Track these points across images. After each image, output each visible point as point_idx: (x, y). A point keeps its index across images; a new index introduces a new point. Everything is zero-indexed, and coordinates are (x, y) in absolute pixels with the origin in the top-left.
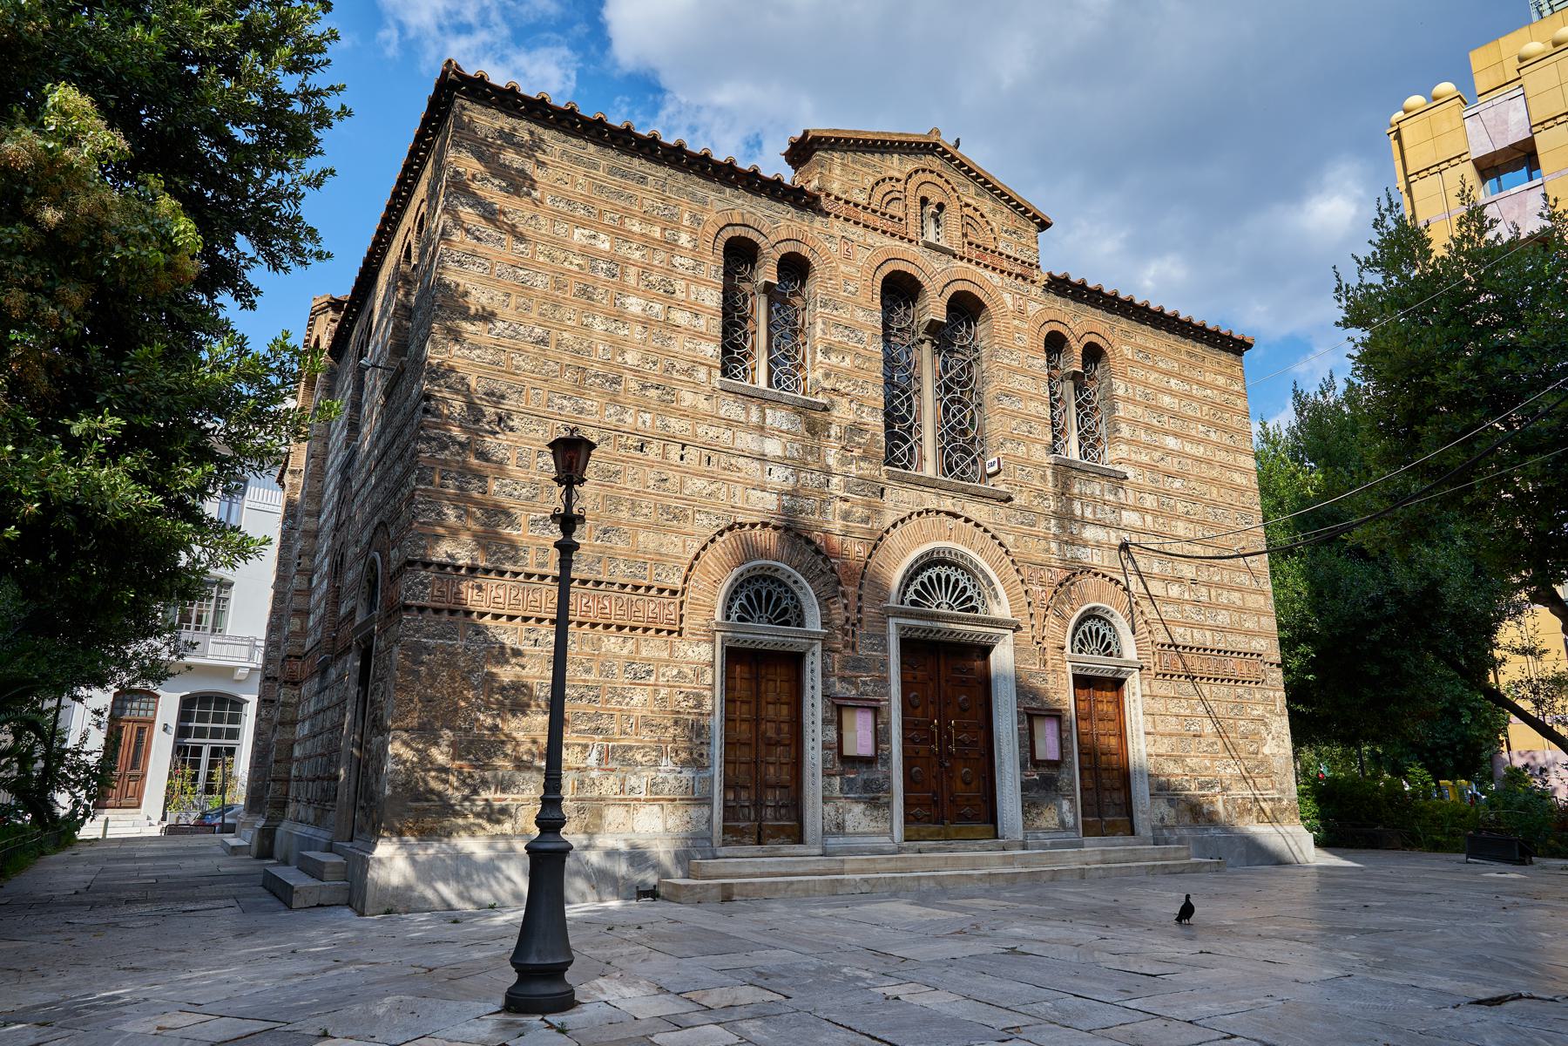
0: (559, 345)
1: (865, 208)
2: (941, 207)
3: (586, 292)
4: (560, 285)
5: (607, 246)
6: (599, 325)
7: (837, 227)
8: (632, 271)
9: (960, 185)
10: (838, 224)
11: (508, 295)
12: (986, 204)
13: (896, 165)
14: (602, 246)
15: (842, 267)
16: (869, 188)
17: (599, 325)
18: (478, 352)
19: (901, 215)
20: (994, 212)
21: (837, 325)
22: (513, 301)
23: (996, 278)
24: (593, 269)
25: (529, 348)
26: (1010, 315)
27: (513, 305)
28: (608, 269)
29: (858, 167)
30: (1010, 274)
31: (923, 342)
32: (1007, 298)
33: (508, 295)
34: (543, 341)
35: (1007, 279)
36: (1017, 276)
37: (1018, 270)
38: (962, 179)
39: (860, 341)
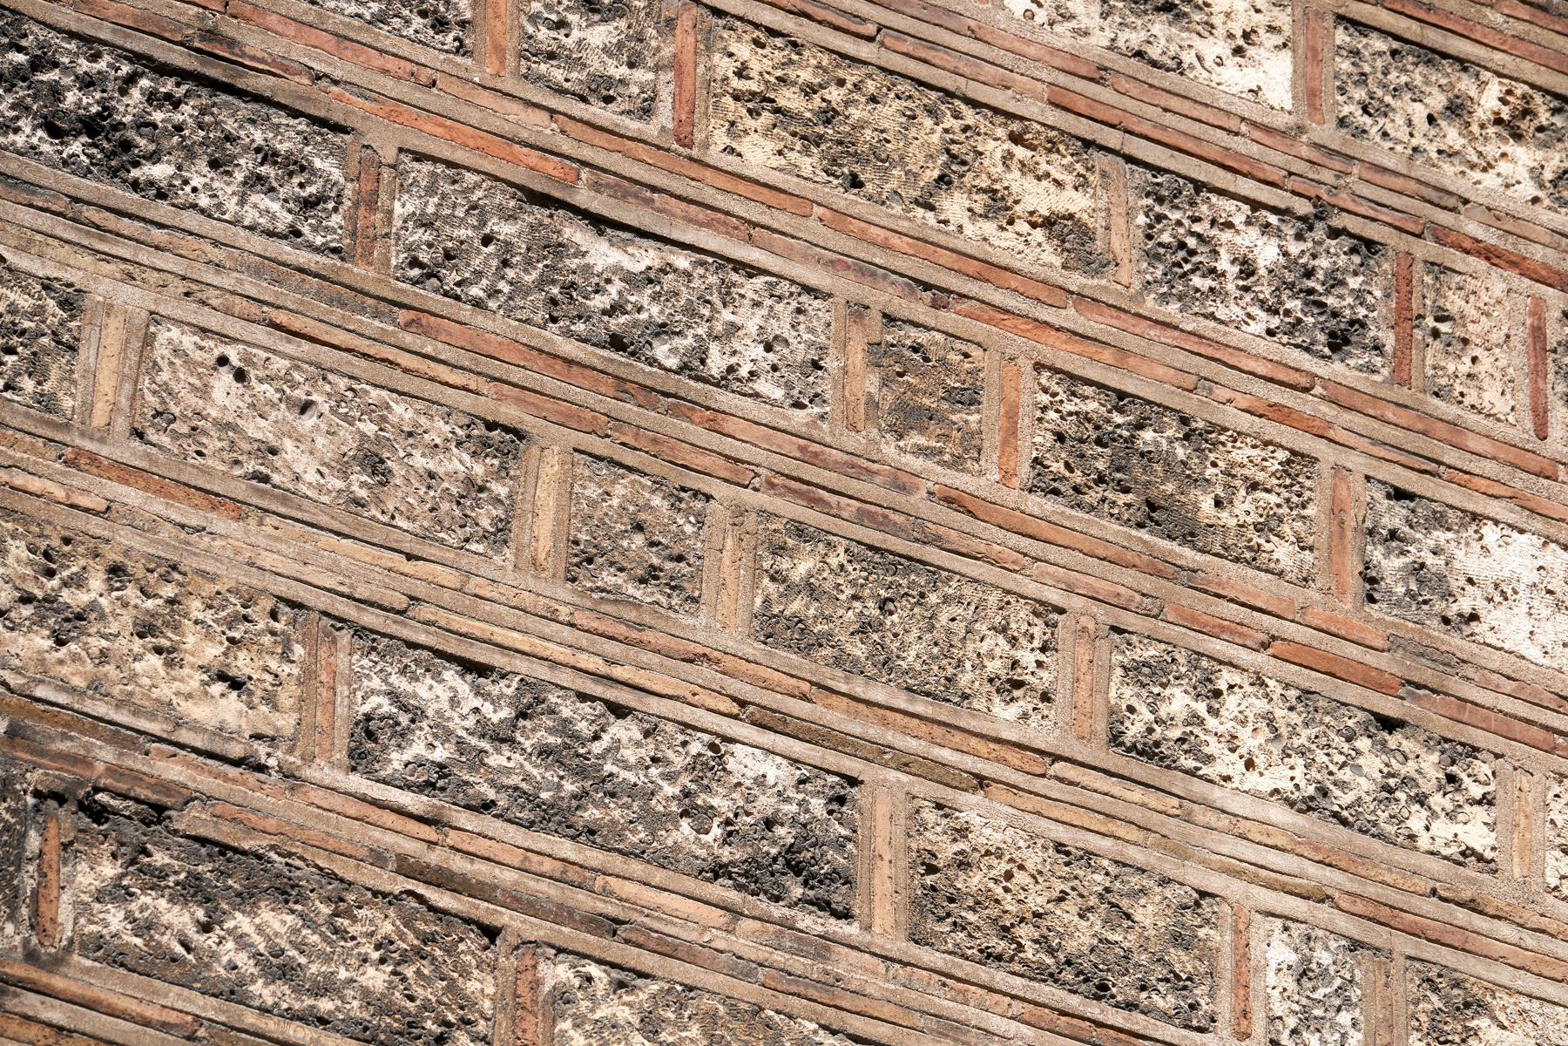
0: (934, 898)
3: (1123, 460)
4: (926, 393)
5: (1272, 78)
6: (1253, 762)
8: (1490, 302)
11: (502, 441)
14: (1234, 78)
17: (1253, 762)
18: (275, 921)
22: (546, 493)
24: (1179, 262)
25: (687, 911)
27: (542, 531)
28: (1297, 278)
33: (502, 441)
34: (795, 869)
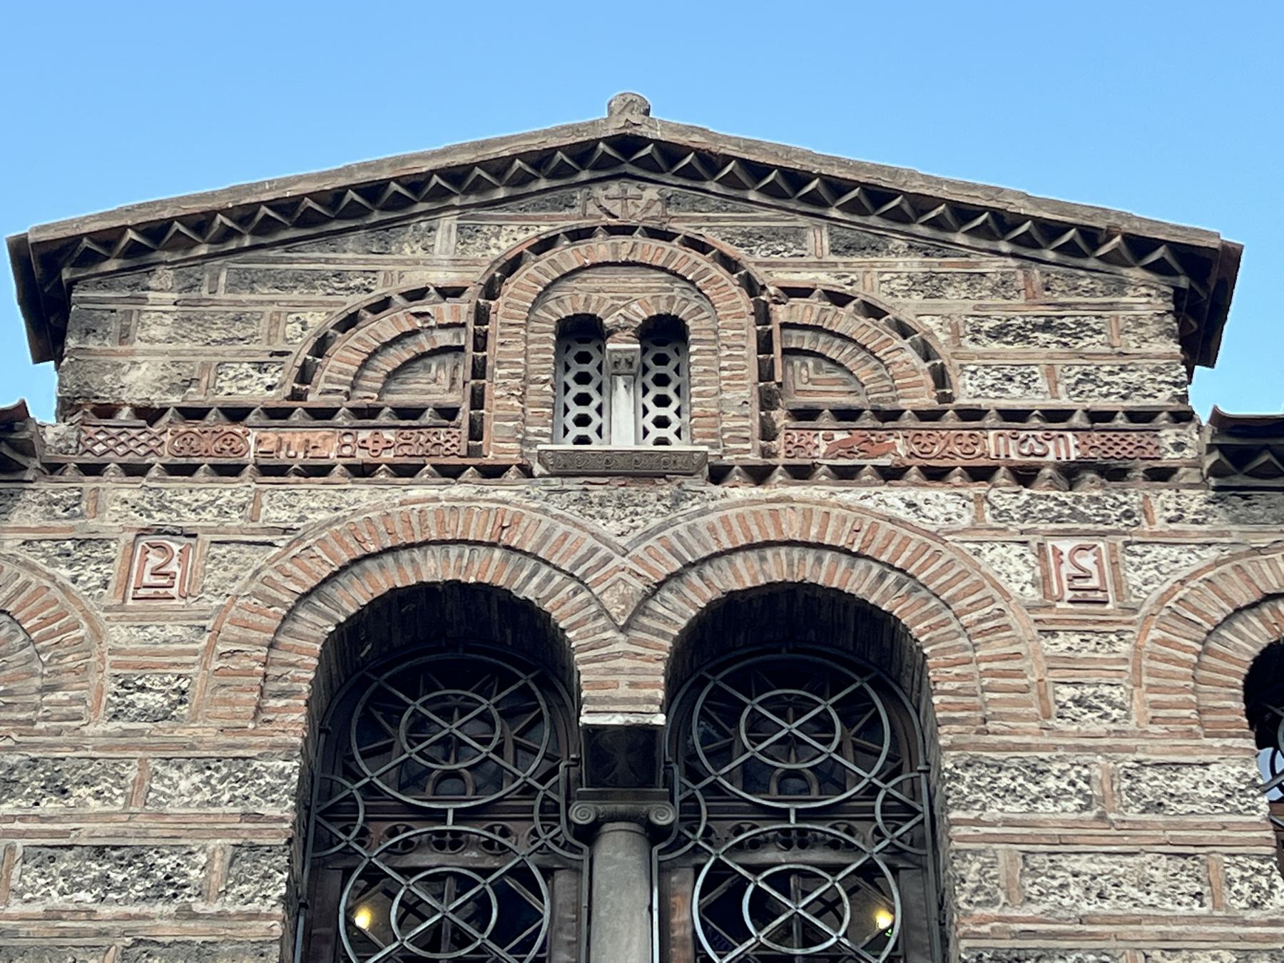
1: (277, 414)
2: (664, 334)
7: (117, 505)
9: (749, 239)
10: (117, 493)
12: (888, 272)
13: (440, 253)
15: (119, 634)
16: (301, 351)
19: (458, 398)
20: (931, 285)
21: (45, 856)
23: (941, 503)
26: (1020, 623)
29: (264, 293)
30: (1025, 476)
31: (589, 834)
32: (1011, 566)
35: (1004, 495)
36: (1070, 473)
37: (1069, 448)
38: (766, 217)
39: (168, 887)
